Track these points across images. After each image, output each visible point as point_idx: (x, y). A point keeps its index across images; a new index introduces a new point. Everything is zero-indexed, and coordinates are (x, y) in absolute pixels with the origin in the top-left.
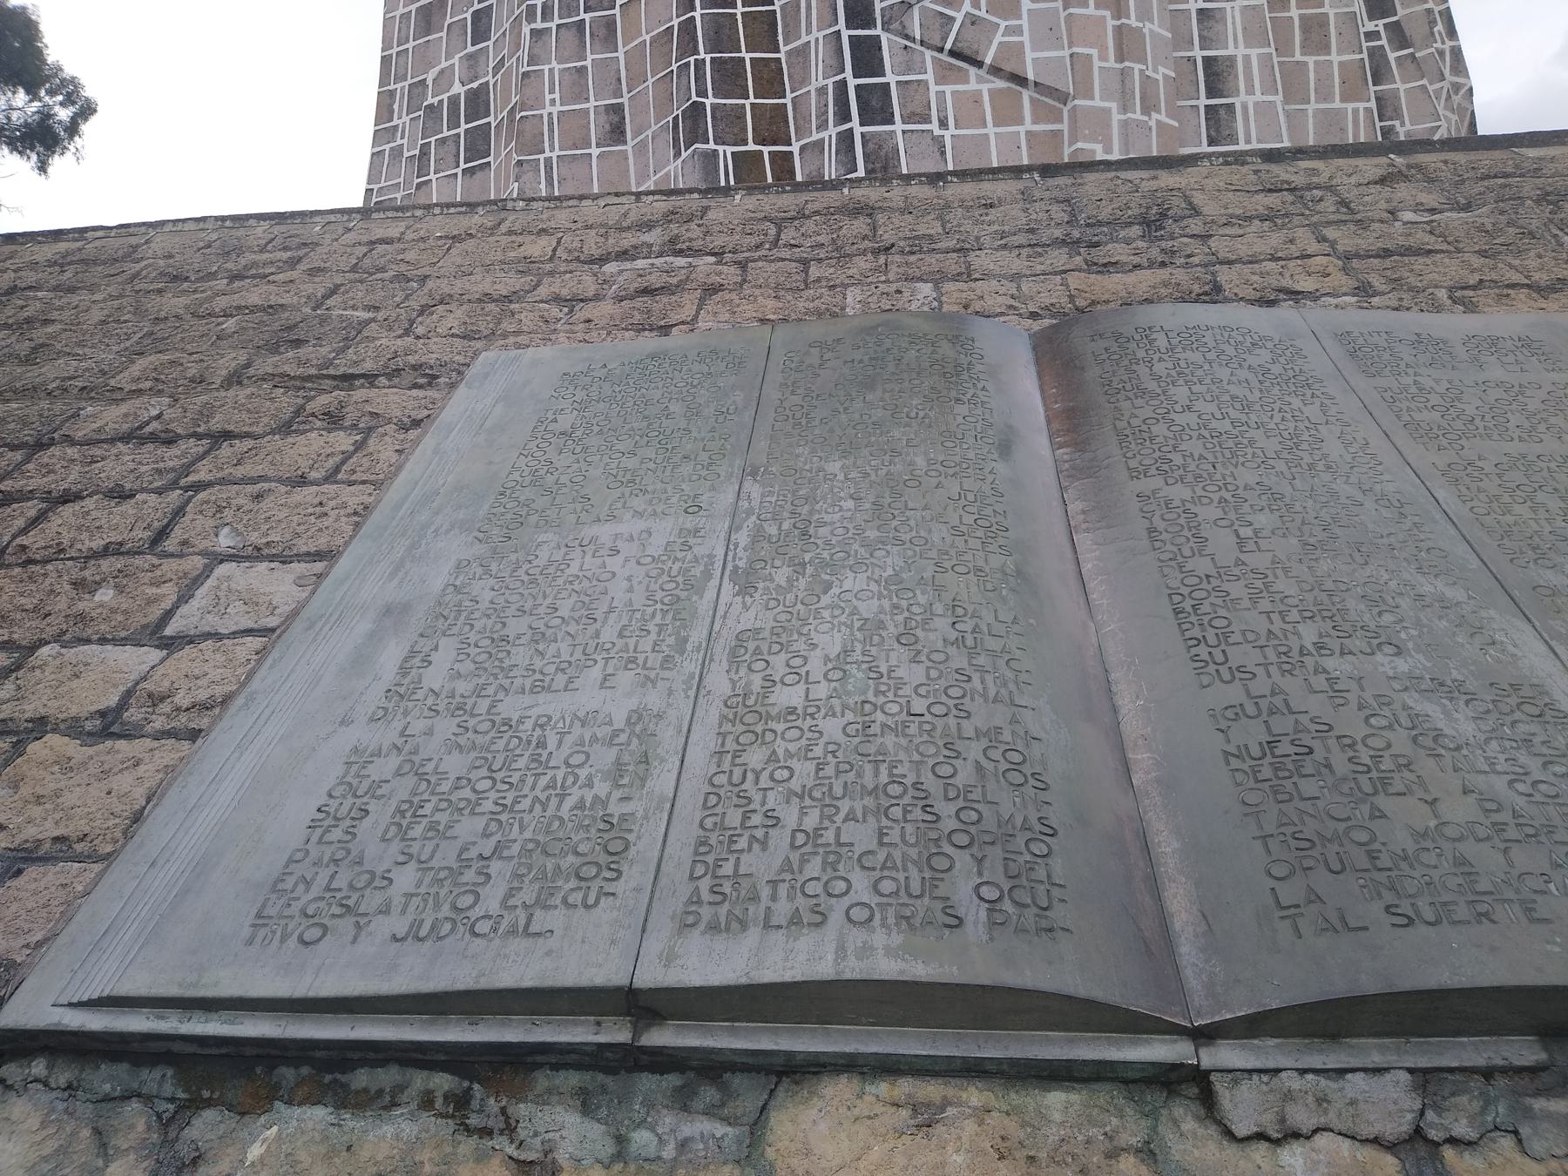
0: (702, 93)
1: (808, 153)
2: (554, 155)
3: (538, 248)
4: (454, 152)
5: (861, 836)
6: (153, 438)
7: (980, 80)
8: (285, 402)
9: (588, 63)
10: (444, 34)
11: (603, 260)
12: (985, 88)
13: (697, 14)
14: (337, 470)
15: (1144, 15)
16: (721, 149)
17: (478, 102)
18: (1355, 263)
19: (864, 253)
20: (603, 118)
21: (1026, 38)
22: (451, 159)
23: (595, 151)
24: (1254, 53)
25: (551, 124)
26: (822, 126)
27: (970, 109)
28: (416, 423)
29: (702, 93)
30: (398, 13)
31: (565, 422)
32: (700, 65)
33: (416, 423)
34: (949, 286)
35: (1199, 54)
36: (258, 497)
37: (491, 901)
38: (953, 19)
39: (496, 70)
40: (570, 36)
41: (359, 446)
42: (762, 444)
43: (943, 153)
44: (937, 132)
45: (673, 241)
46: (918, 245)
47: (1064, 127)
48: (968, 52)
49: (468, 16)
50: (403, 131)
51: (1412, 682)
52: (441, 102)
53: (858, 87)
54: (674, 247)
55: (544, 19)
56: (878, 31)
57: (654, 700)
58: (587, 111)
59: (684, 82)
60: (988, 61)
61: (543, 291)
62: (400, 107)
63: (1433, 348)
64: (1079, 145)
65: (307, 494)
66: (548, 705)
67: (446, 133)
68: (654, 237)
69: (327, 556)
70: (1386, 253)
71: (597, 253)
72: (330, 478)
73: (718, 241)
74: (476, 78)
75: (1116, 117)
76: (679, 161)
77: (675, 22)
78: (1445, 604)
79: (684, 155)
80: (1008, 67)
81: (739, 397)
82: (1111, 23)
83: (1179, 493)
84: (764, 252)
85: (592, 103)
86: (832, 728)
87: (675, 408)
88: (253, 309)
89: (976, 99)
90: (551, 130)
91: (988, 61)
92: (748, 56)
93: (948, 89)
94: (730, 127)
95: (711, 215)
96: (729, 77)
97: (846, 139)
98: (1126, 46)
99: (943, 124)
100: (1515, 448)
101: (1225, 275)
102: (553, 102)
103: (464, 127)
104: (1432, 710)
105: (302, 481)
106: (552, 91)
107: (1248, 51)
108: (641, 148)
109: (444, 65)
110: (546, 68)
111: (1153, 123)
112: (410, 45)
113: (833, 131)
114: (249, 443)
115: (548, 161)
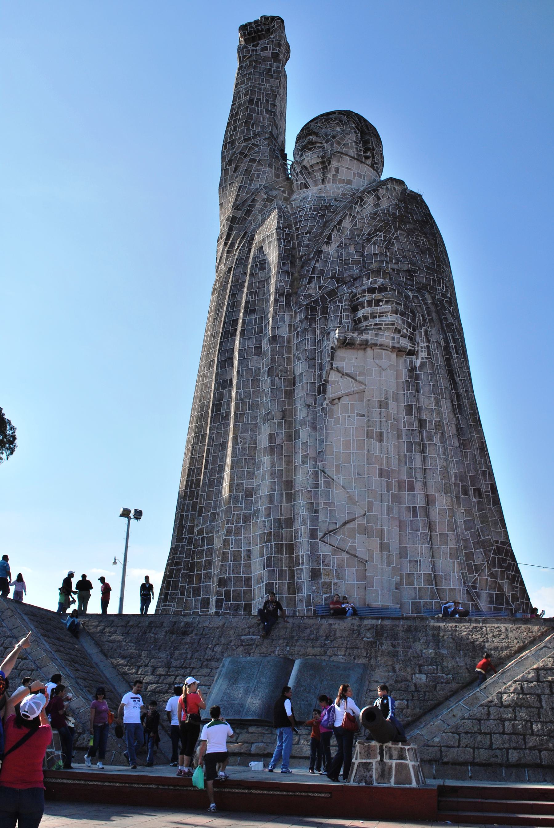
6: (184, 667)
14: (209, 674)
36: (201, 678)
41: (211, 671)
65: (206, 678)
69: (210, 686)
72: (209, 675)
80: (351, 552)
88: (190, 643)
105: (205, 676)
109: (201, 527)
114: (197, 670)
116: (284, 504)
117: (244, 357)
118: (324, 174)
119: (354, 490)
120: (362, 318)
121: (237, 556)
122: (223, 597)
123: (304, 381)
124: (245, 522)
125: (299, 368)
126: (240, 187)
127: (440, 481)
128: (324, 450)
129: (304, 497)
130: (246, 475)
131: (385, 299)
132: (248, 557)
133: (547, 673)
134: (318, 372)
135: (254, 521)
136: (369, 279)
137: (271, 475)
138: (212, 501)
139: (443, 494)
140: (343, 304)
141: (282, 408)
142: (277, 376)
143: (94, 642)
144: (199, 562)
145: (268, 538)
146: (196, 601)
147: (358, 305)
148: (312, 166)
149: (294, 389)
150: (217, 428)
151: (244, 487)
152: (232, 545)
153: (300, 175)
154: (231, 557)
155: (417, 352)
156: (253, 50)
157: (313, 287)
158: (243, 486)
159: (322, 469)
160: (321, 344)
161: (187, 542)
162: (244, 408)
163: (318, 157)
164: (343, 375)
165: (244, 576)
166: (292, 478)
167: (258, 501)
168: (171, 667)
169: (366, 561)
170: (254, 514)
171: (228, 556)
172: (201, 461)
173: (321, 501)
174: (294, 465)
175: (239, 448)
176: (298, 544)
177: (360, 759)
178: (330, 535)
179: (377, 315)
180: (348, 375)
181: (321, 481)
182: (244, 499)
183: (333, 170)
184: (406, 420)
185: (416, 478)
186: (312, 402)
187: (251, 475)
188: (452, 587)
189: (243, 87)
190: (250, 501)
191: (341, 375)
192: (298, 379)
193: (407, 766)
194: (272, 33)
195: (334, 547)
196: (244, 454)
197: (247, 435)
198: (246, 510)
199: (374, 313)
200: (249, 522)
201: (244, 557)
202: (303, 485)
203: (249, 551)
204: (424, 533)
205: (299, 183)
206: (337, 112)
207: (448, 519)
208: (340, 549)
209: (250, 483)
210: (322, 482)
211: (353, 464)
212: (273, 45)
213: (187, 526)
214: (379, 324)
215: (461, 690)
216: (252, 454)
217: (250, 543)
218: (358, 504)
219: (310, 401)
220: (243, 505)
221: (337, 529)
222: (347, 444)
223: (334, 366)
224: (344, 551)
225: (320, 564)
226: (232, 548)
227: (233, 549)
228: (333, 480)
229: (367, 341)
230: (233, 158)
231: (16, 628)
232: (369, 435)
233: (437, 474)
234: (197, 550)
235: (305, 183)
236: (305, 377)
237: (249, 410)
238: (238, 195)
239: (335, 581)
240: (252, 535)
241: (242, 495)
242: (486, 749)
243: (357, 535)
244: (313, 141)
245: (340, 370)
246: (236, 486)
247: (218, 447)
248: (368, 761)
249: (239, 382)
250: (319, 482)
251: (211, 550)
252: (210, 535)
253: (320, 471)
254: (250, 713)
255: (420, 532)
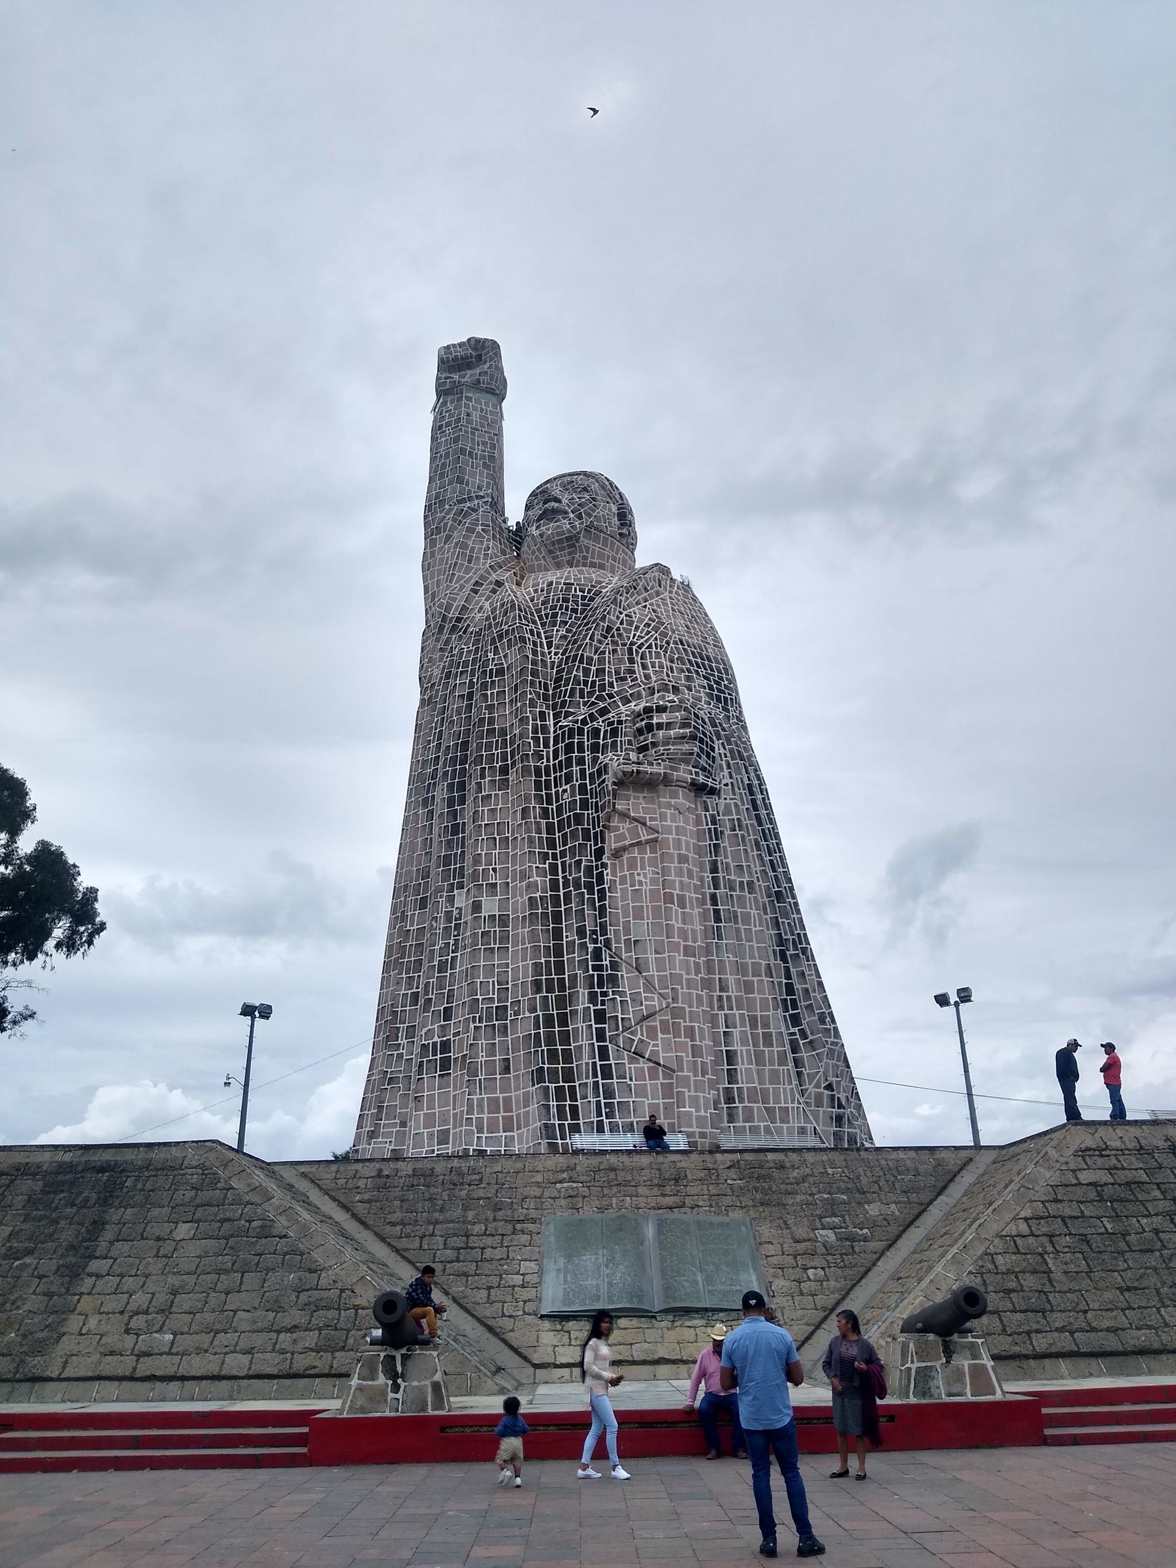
0: (543, 1063)
1: (581, 1087)
2: (482, 1078)
3: (539, 1178)
4: (434, 1066)
5: (625, 1296)
7: (644, 1063)
8: (510, 1227)
9: (497, 1041)
10: (430, 1014)
11: (556, 1183)
12: (646, 1066)
13: (541, 1031)
15: (702, 1039)
16: (550, 1085)
17: (445, 1047)
18: (713, 1198)
19: (615, 1185)
20: (502, 1063)
21: (660, 1048)
22: (434, 1070)
23: (498, 1077)
24: (744, 1048)
25: (481, 1065)
26: (587, 1077)
27: (640, 1075)
28: (539, 1233)
29: (543, 1063)
30: (401, 993)
31: (570, 1235)
32: (543, 1051)
33: (539, 1233)
34: (634, 1198)
35: (724, 1049)
37: (587, 1302)
38: (634, 1040)
39: (455, 1035)
40: (489, 1030)
42: (604, 1242)
43: (631, 1091)
44: (629, 1083)
45: (571, 1178)
46: (626, 1184)
47: (674, 1081)
48: (639, 1053)
49: (442, 1008)
50: (403, 1046)
51: (684, 1280)
52: (429, 1043)
53: (600, 1065)
54: (571, 1180)
55: (479, 1023)
56: (607, 1043)
57: (599, 1282)
58: (495, 1060)
59: (536, 1057)
60: (647, 1056)
61: (546, 1194)
62: (402, 1035)
63: (711, 1224)
64: (679, 1089)
66: (586, 1283)
67: (431, 1058)
68: (565, 1175)
70: (718, 1195)
71: (554, 1181)
73: (582, 1178)
74: (445, 1036)
75: (692, 1078)
76: (534, 1088)
77: (533, 1032)
78: (692, 1271)
79: (536, 1086)
81: (599, 1231)
82: (690, 1043)
83: (665, 1253)
84: (592, 1183)
85: (498, 1057)
86: (620, 1285)
87: (588, 1233)
89: (643, 1071)
90: (481, 1067)
91: (647, 1056)
92: (560, 1048)
93: (632, 1066)
94: (553, 1074)
95: (578, 1168)
96: (553, 1056)
97: (596, 1084)
98: (696, 1052)
99: (631, 1080)
100: (712, 1246)
101: (688, 1201)
102: (482, 1056)
103: (439, 1056)
104: (685, 1283)
106: (482, 1052)
107: (742, 1048)
108: (517, 1077)
109: (430, 1027)
110: (480, 1042)
111: (706, 1080)
112: (408, 1008)
113: (591, 1080)
115: (480, 1080)
133: (1040, 1223)
140: (624, 726)
143: (336, 1203)
146: (431, 1135)
155: (720, 790)
168: (469, 1236)
175: (485, 917)
177: (918, 1362)
193: (984, 1367)
194: (485, 362)
215: (888, 1250)
230: (442, 524)
231: (255, 1189)
242: (999, 1335)
248: (929, 1364)
254: (615, 1299)
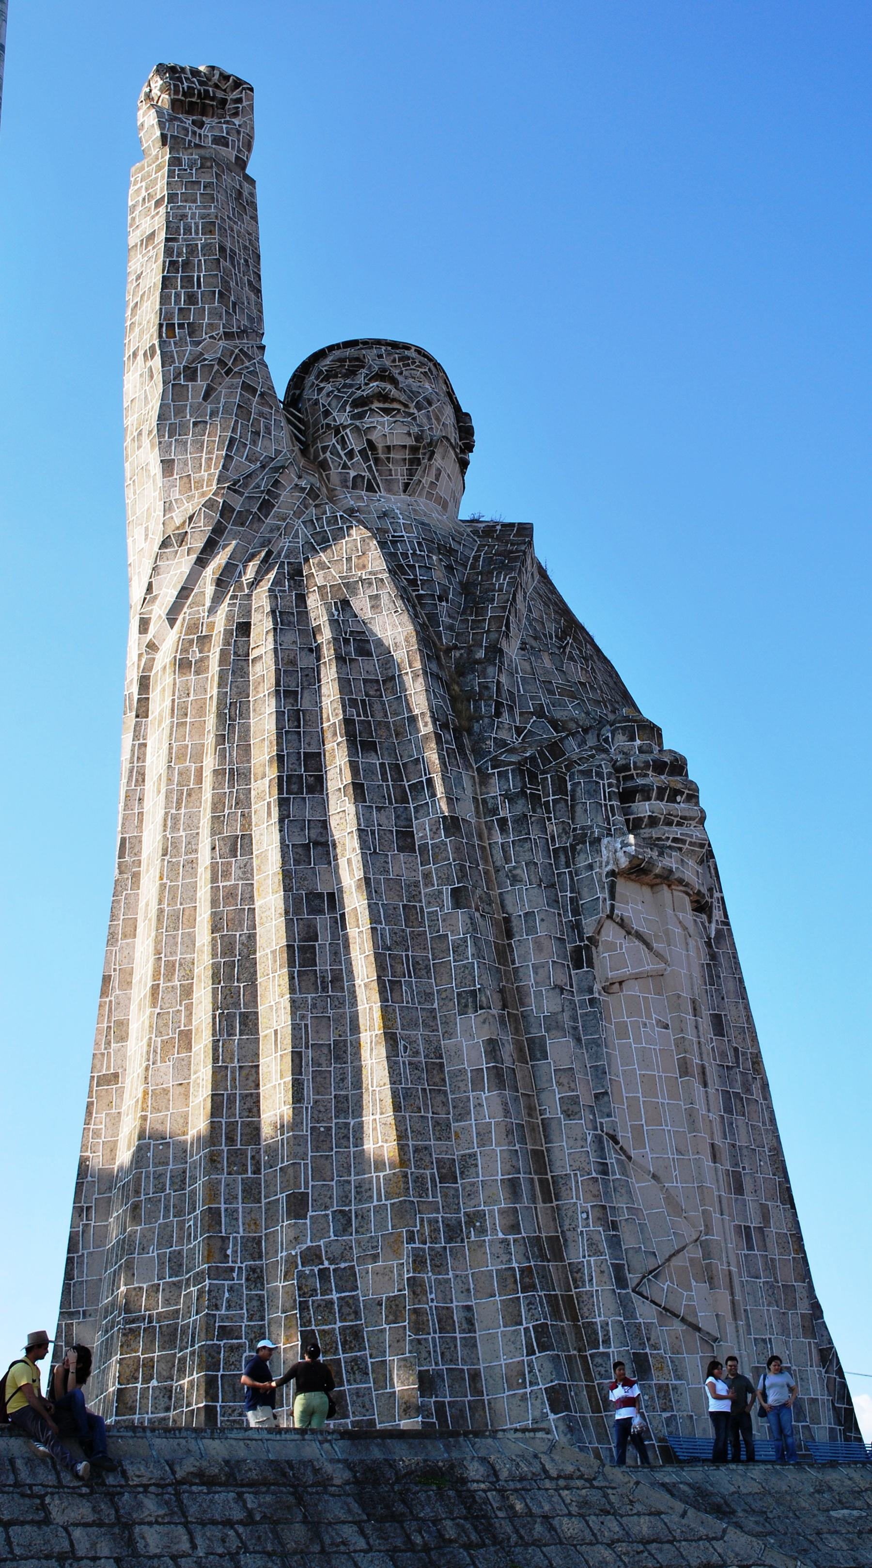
116: (540, 1205)
117: (375, 849)
118: (411, 473)
119: (675, 1184)
120: (646, 820)
121: (445, 1320)
122: (434, 1420)
123: (542, 931)
124: (449, 1240)
125: (521, 899)
126: (232, 441)
127: (771, 1176)
128: (609, 1091)
129: (585, 1192)
130: (434, 1130)
131: (686, 791)
132: (467, 1323)
134: (566, 916)
135: (473, 1239)
136: (632, 739)
137: (507, 1136)
138: (334, 1183)
139: (779, 1204)
141: (499, 985)
142: (477, 910)
144: (323, 1330)
145: (527, 1280)
147: (637, 791)
148: (388, 448)
149: (510, 945)
150: (314, 1006)
151: (434, 1156)
152: (431, 1293)
153: (358, 458)
154: (433, 1322)
156: (194, 133)
157: (507, 726)
158: (431, 1155)
159: (611, 1132)
160: (567, 857)
161: (247, 1280)
162: (398, 968)
163: (409, 434)
164: (629, 933)
165: (465, 1368)
166: (542, 1146)
167: (477, 1192)
169: (715, 1340)
170: (470, 1222)
171: (428, 1320)
172: (251, 1078)
173: (621, 1204)
174: (540, 1118)
176: (585, 1298)
178: (649, 1280)
179: (676, 819)
180: (639, 936)
181: (612, 1159)
182: (439, 1185)
183: (434, 472)
184: (714, 1044)
185: (744, 1169)
186: (564, 980)
187: (443, 1129)
188: (812, 1396)
189: (193, 211)
190: (452, 1192)
191: (624, 933)
192: (519, 925)
195: (660, 1306)
196: (419, 1078)
197: (419, 1034)
198: (447, 1210)
199: (671, 815)
200: (459, 1239)
201: (461, 1323)
202: (576, 1165)
203: (469, 1308)
204: (767, 1282)
205: (353, 474)
206: (413, 348)
207: (793, 1255)
208: (671, 1312)
209: (444, 1148)
210: (614, 1161)
211: (666, 1128)
212: (239, 141)
213: (235, 1238)
214: (682, 840)
216: (437, 1079)
217: (468, 1290)
218: (685, 1215)
219: (561, 978)
220: (439, 1199)
221: (659, 1266)
222: (649, 1083)
223: (616, 911)
224: (677, 1316)
225: (644, 1343)
226: (432, 1301)
227: (435, 1304)
228: (629, 1158)
229: (671, 871)
232: (684, 1069)
233: (766, 1163)
234: (313, 1302)
235: (369, 480)
236: (545, 924)
237: (410, 977)
238: (228, 457)
239: (674, 1382)
240: (470, 1272)
241: (433, 1175)
243: (694, 1283)
244: (391, 396)
245: (626, 920)
246: (414, 1152)
247: (325, 1051)
249: (373, 906)
250: (608, 1161)
251: (351, 1301)
252: (343, 1265)
253: (605, 1137)
255: (762, 1281)
